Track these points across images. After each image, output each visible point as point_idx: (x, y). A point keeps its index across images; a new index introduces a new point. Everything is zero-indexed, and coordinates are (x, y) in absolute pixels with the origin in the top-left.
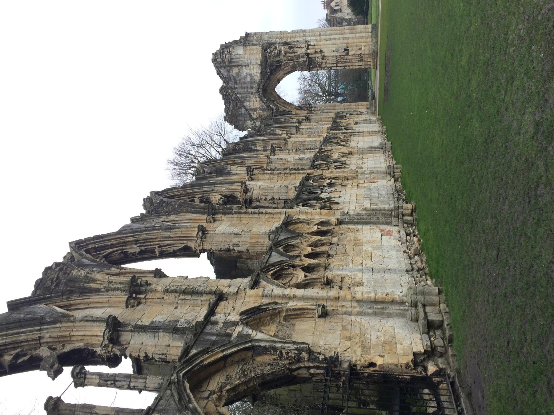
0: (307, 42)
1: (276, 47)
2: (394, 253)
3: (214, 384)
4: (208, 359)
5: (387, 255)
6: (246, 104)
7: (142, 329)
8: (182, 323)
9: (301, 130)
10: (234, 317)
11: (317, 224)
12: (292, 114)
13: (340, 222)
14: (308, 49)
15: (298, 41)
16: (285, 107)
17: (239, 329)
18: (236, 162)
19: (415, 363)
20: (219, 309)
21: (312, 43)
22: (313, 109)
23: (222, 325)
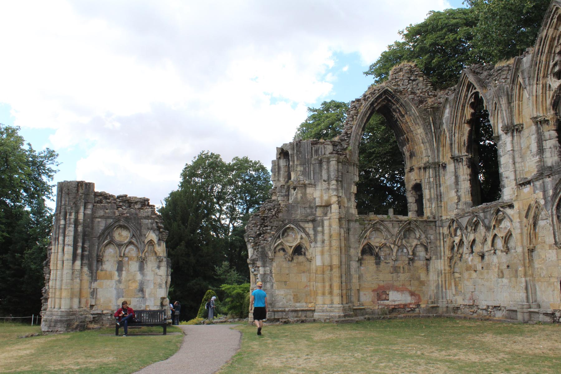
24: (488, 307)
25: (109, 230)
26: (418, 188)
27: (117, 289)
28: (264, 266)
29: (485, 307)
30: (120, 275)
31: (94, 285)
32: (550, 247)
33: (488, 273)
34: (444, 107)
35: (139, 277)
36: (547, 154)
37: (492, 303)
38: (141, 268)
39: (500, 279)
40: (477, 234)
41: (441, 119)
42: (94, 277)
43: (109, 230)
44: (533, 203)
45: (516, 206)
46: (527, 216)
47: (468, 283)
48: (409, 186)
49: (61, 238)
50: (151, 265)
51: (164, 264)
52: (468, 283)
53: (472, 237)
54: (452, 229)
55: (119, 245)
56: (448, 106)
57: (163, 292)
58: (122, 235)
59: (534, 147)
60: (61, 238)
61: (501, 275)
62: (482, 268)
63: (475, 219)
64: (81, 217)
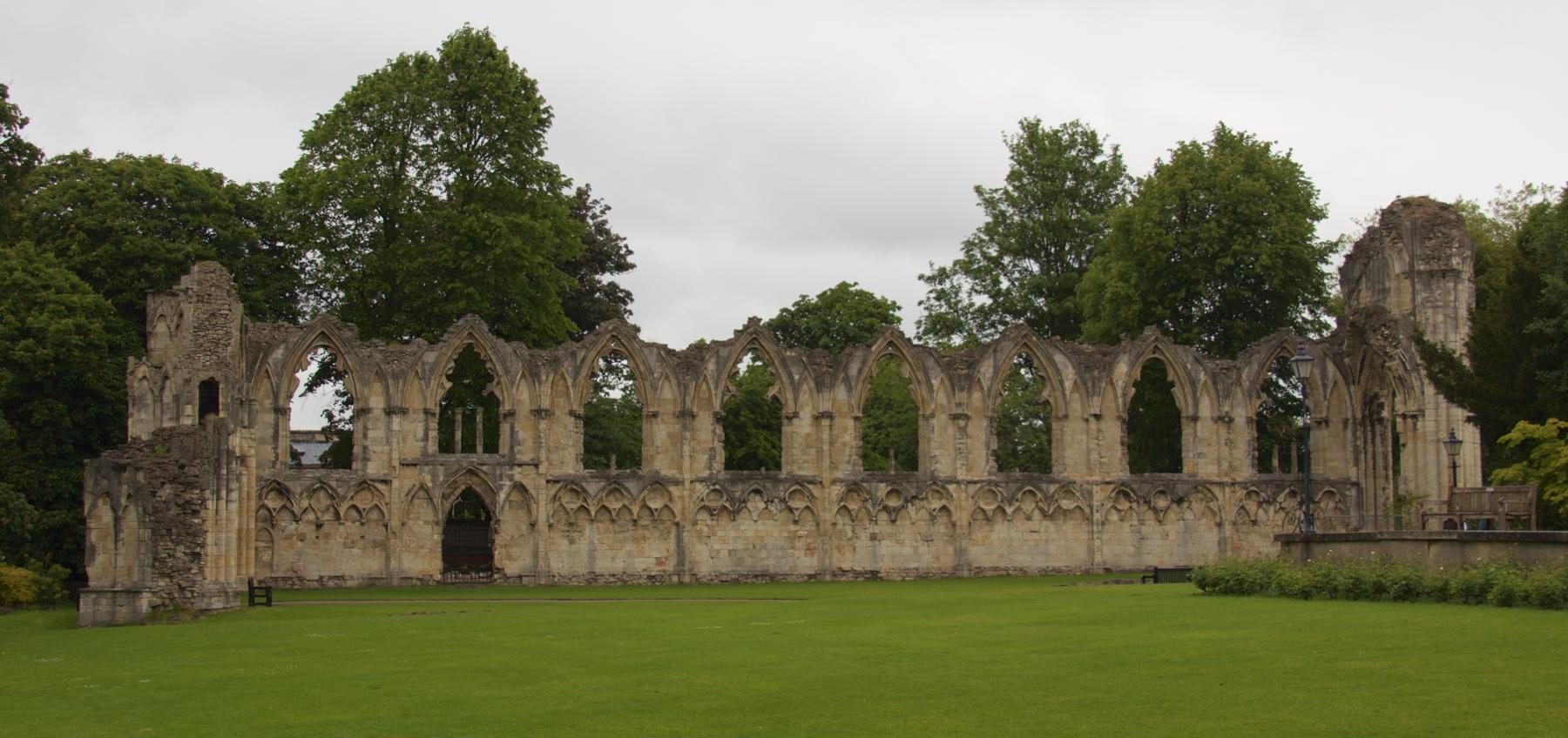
0: (1422, 412)
1: (1396, 347)
2: (622, 565)
3: (475, 479)
4: (483, 475)
5: (618, 560)
6: (1364, 279)
7: (512, 428)
8: (516, 449)
9: (1192, 424)
10: (517, 478)
11: (666, 506)
12: (1347, 384)
13: (677, 524)
14: (1404, 416)
15: (1423, 393)
16: (1361, 372)
17: (508, 483)
18: (918, 373)
19: (497, 568)
20: (525, 467)
21: (1419, 424)
22: (1369, 428)
23: (510, 473)
24: (321, 578)
29: (317, 578)
32: (426, 523)
33: (326, 543)
34: (278, 347)
36: (430, 443)
37: (326, 573)
39: (346, 550)
40: (313, 502)
41: (266, 355)
44: (417, 483)
45: (396, 484)
46: (407, 495)
47: (284, 553)
49: (224, 493)
52: (284, 553)
53: (305, 503)
54: (265, 490)
56: (283, 346)
59: (420, 434)
61: (349, 544)
62: (317, 537)
63: (318, 485)
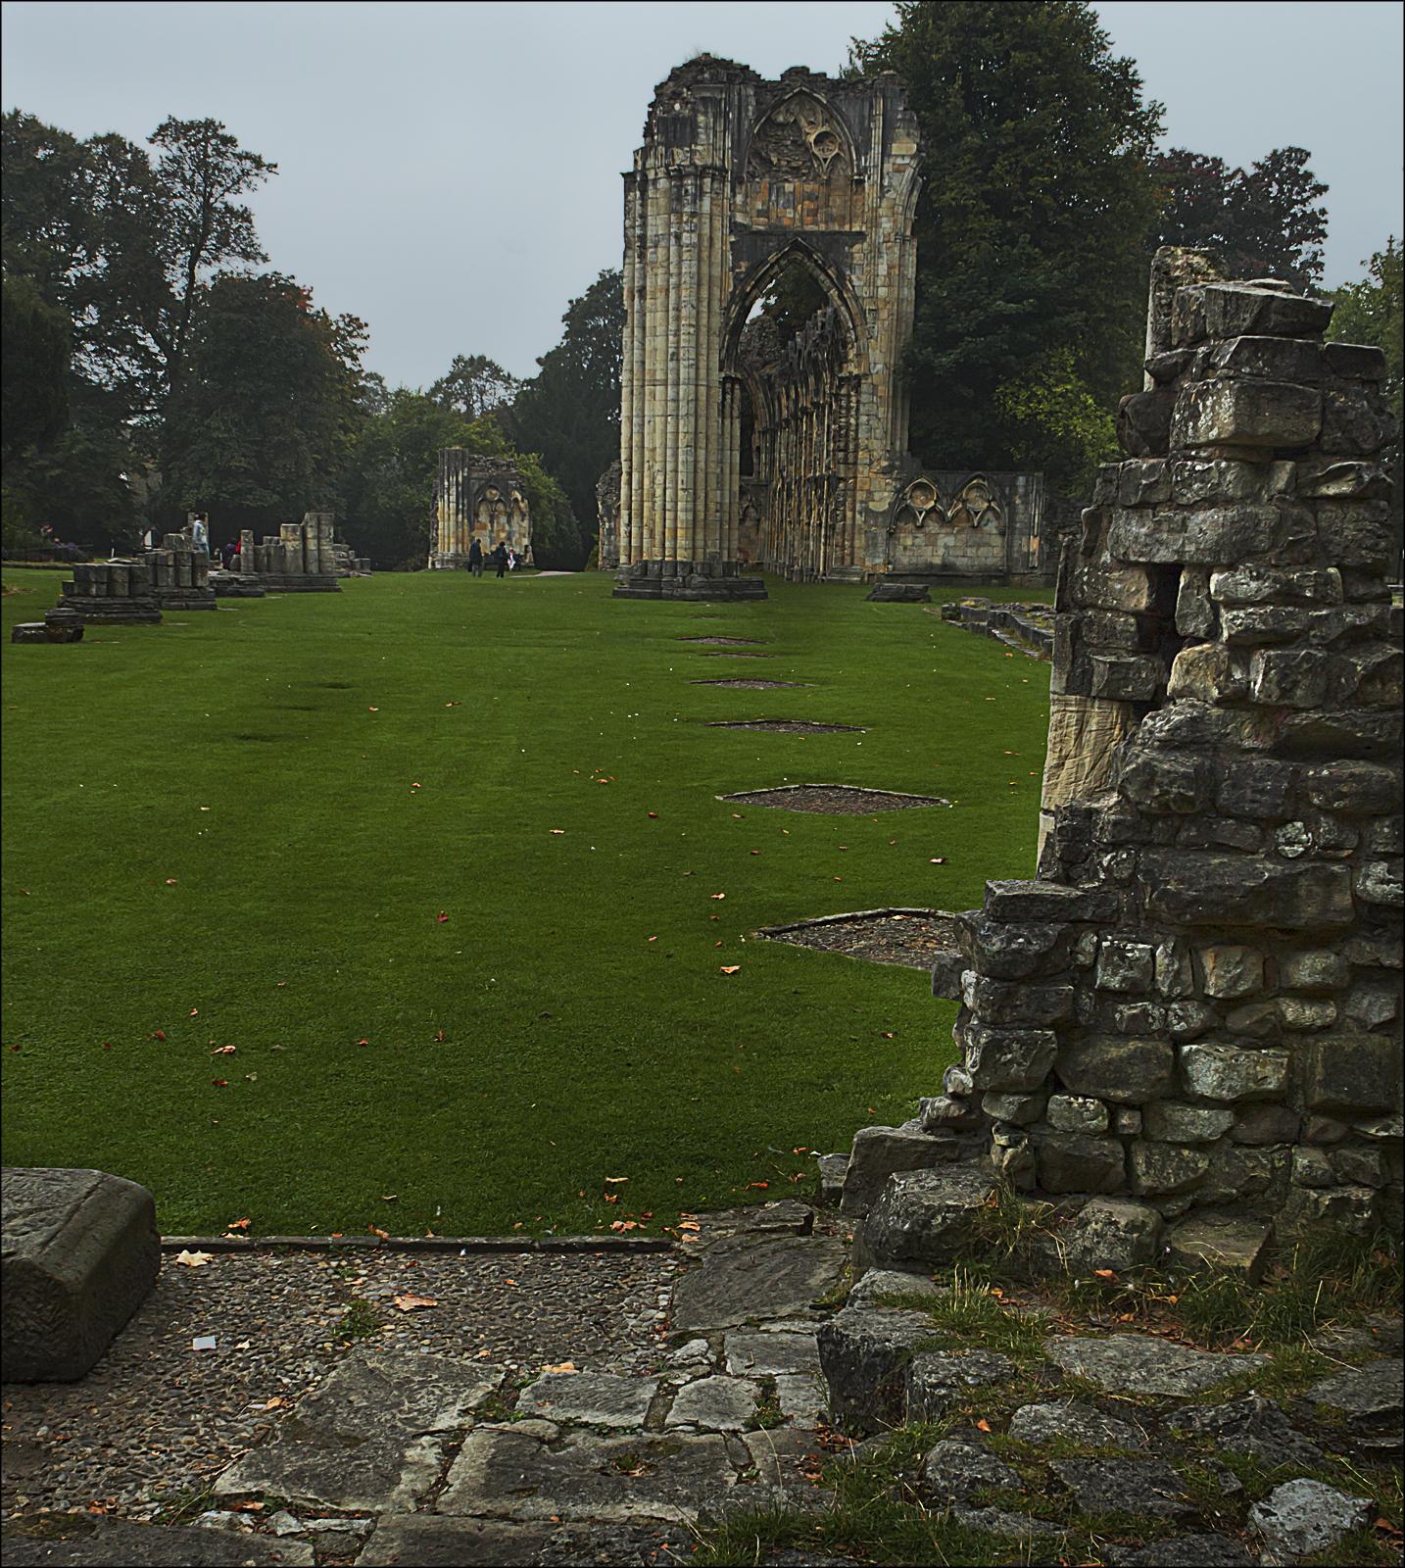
25: (481, 490)
26: (758, 448)
27: (490, 537)
28: (610, 522)
30: (492, 526)
31: (473, 534)
35: (507, 528)
38: (509, 522)
42: (472, 529)
43: (481, 490)
48: (754, 447)
49: (446, 497)
50: (516, 518)
51: (527, 517)
55: (491, 502)
57: (526, 541)
58: (493, 494)
60: (446, 497)
64: (460, 479)
